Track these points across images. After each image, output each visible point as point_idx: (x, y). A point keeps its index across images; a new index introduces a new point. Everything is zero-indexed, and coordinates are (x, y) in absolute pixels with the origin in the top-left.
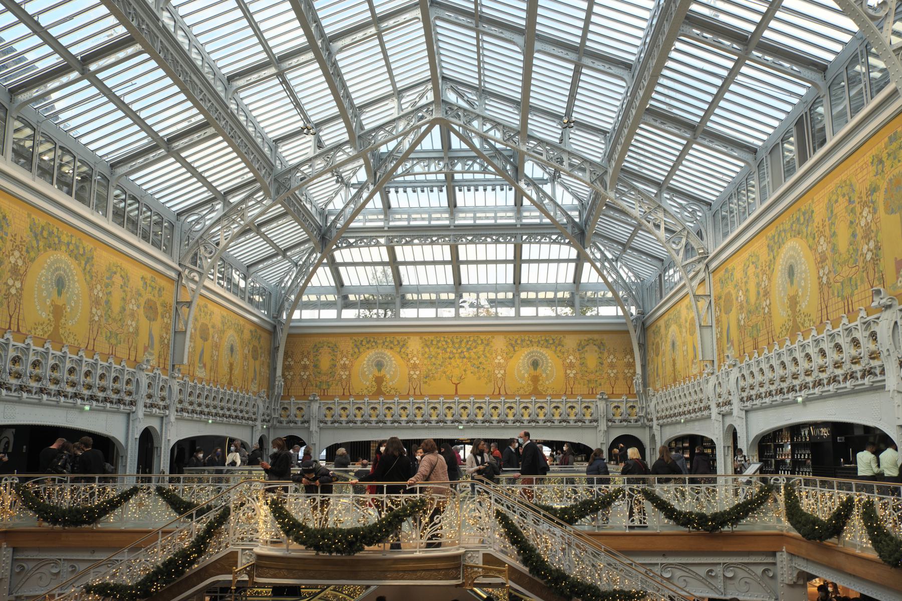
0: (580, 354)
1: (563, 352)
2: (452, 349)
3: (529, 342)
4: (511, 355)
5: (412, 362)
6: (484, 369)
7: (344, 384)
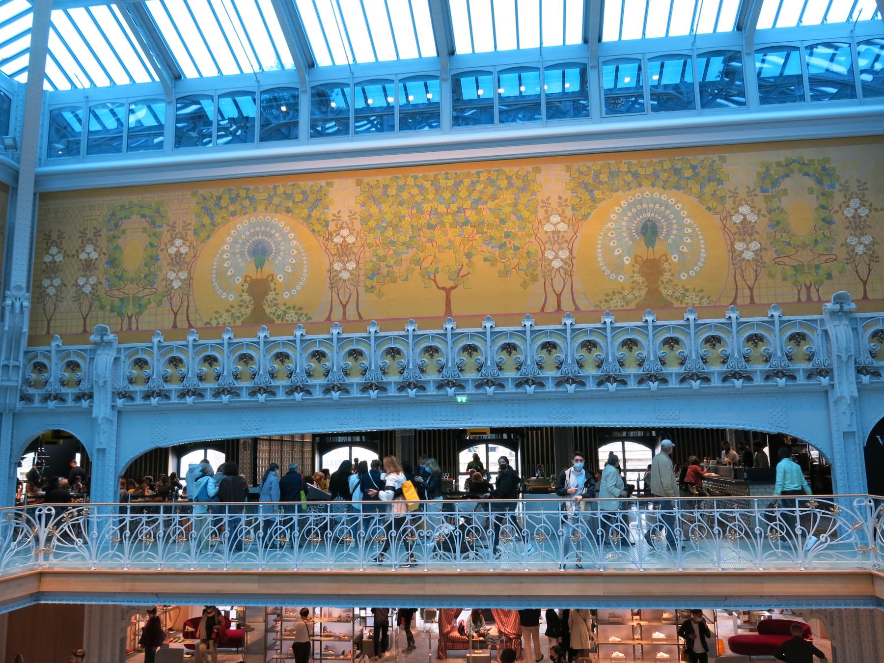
0: (768, 199)
1: (722, 199)
2: (435, 204)
3: (629, 178)
4: (584, 211)
5: (338, 240)
6: (516, 248)
7: (176, 301)
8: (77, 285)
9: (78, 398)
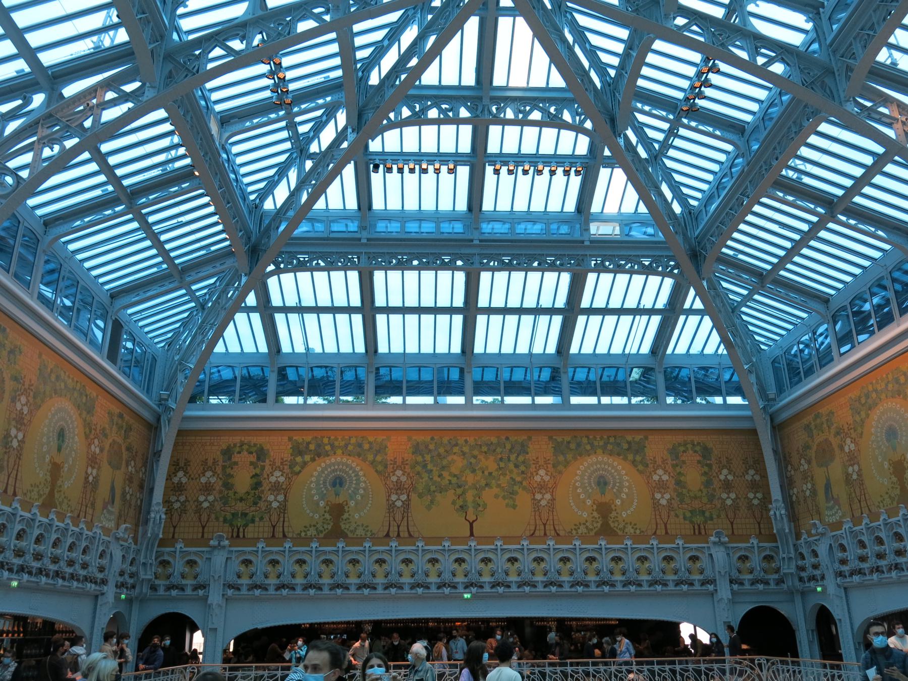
7: (274, 518)
8: (197, 500)
9: (196, 588)
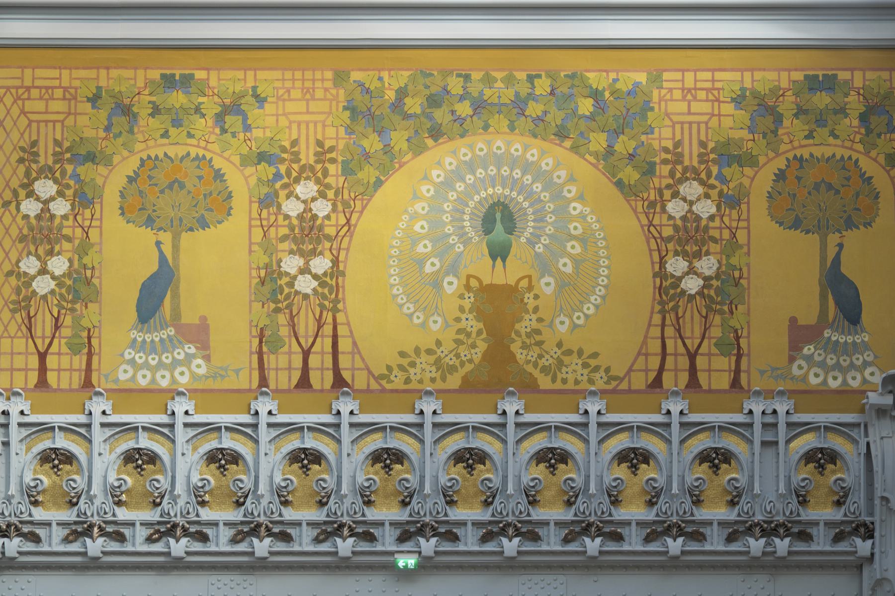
7: (306, 324)
